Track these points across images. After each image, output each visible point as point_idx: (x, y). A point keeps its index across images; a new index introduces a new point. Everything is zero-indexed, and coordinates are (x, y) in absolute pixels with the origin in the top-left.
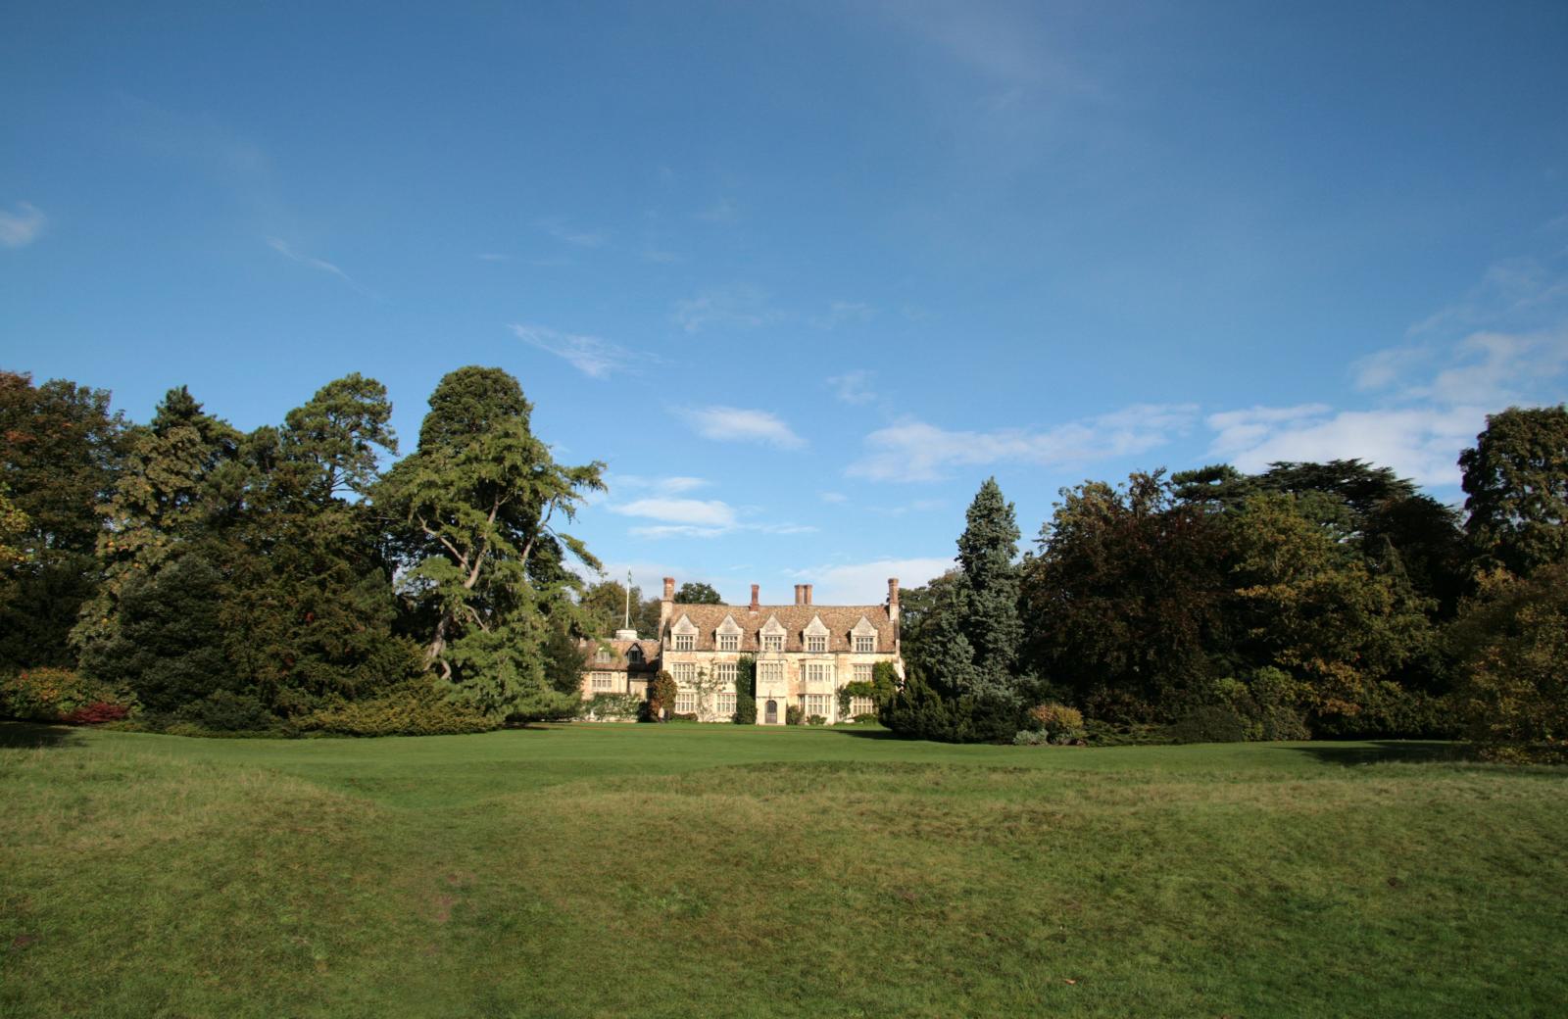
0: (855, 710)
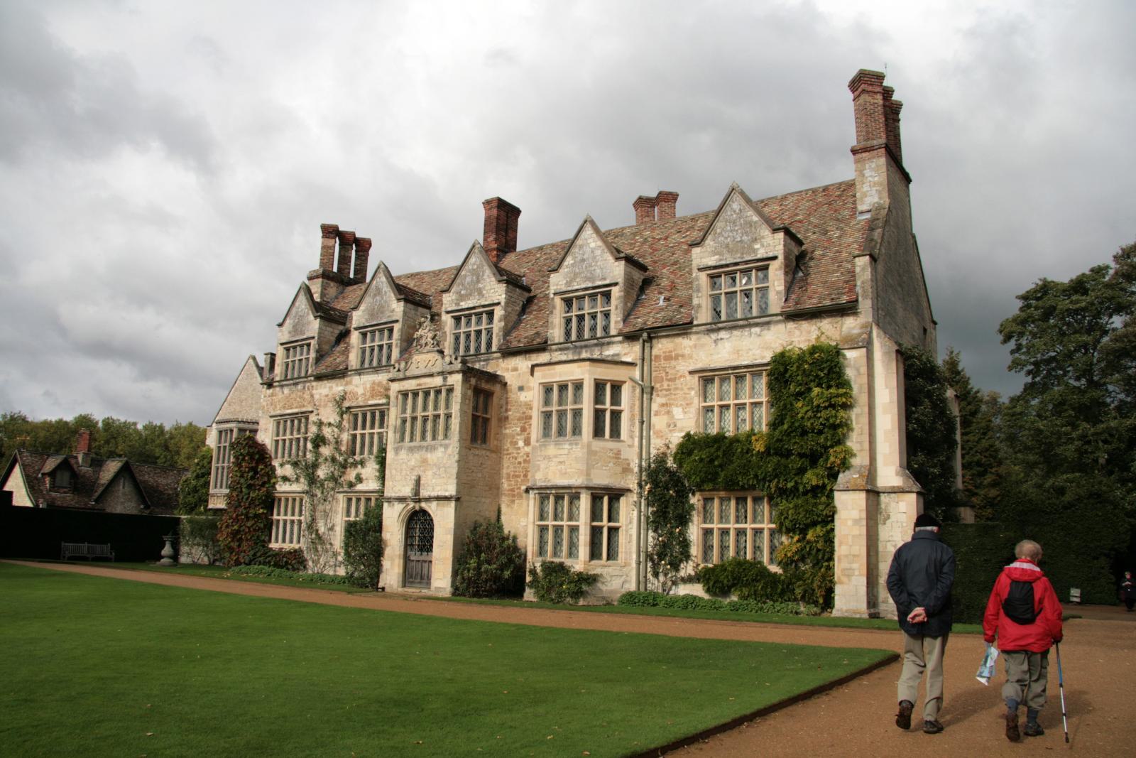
0: (707, 549)
